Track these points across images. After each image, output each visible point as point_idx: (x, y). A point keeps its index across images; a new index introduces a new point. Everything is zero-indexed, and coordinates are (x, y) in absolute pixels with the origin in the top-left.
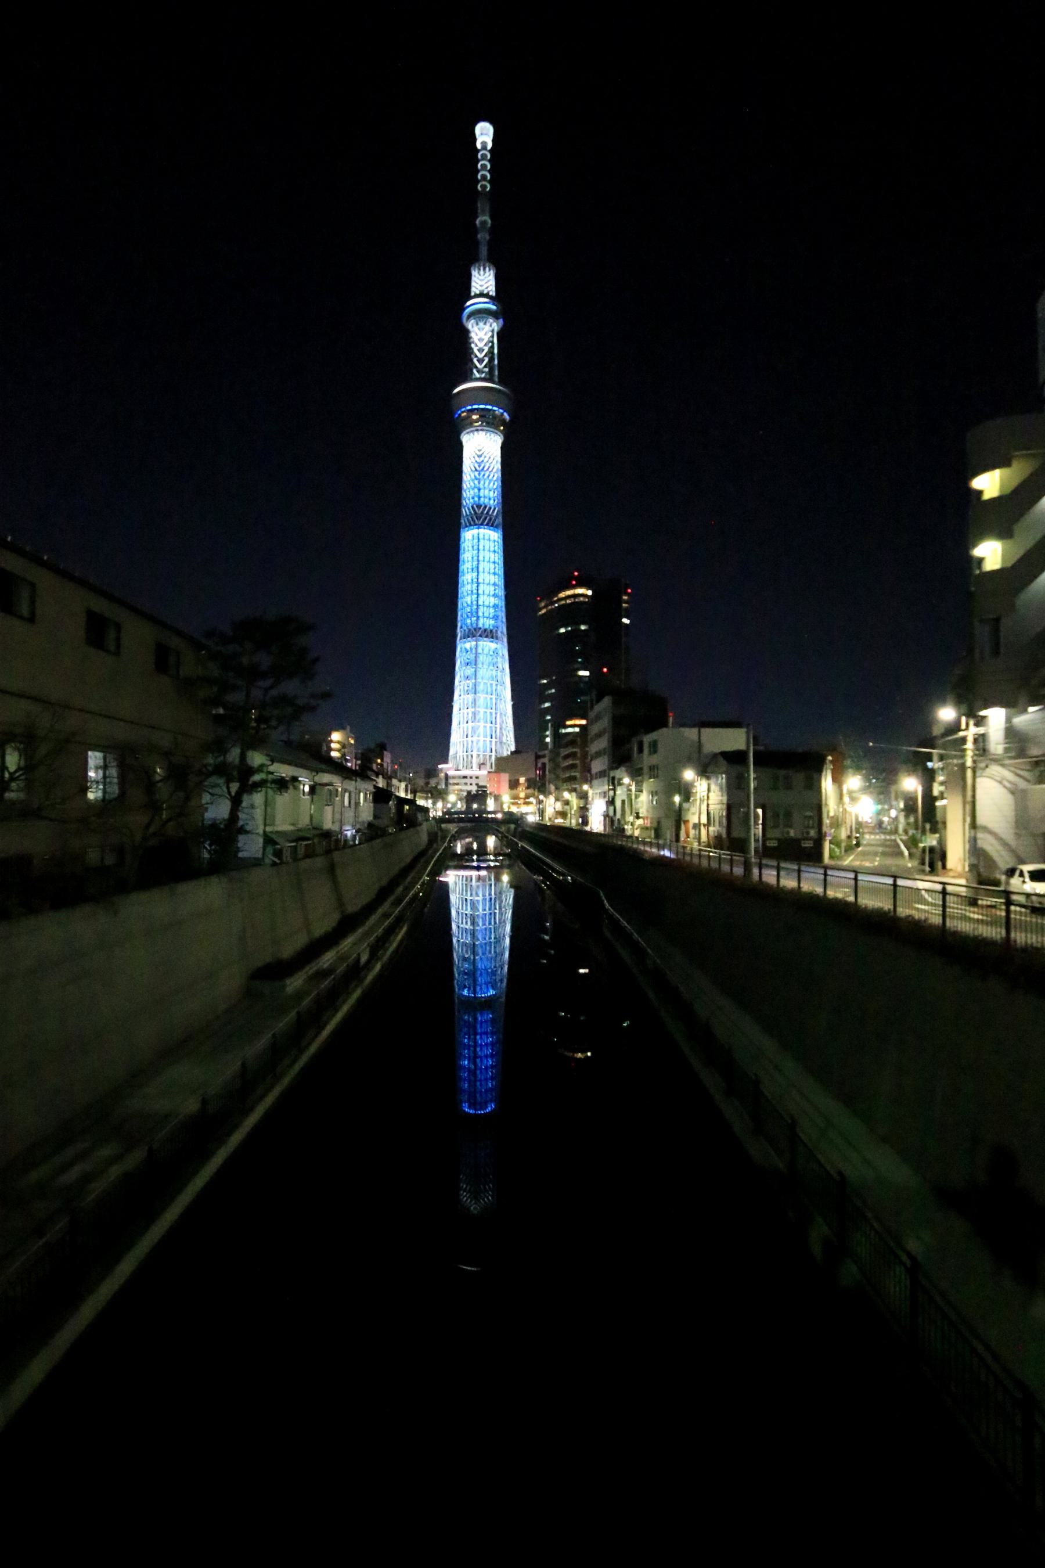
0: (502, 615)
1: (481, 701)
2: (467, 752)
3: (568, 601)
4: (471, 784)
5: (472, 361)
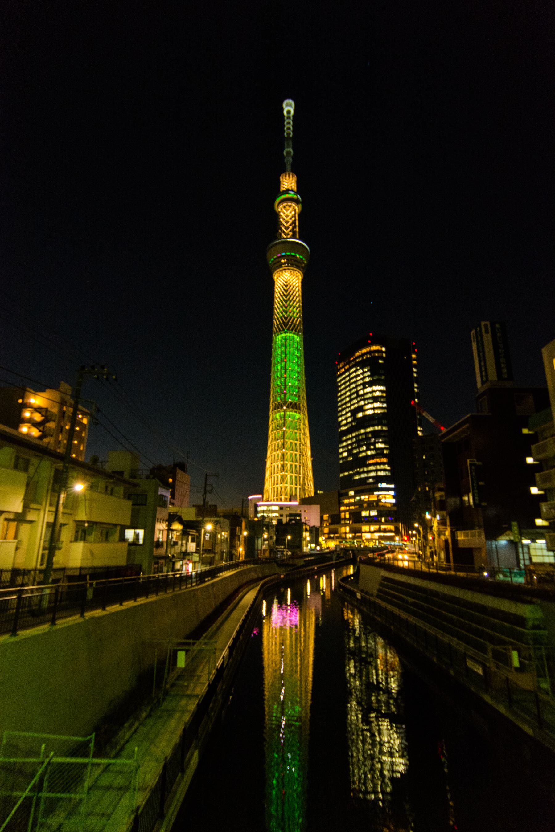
0: (303, 394)
2: (277, 496)
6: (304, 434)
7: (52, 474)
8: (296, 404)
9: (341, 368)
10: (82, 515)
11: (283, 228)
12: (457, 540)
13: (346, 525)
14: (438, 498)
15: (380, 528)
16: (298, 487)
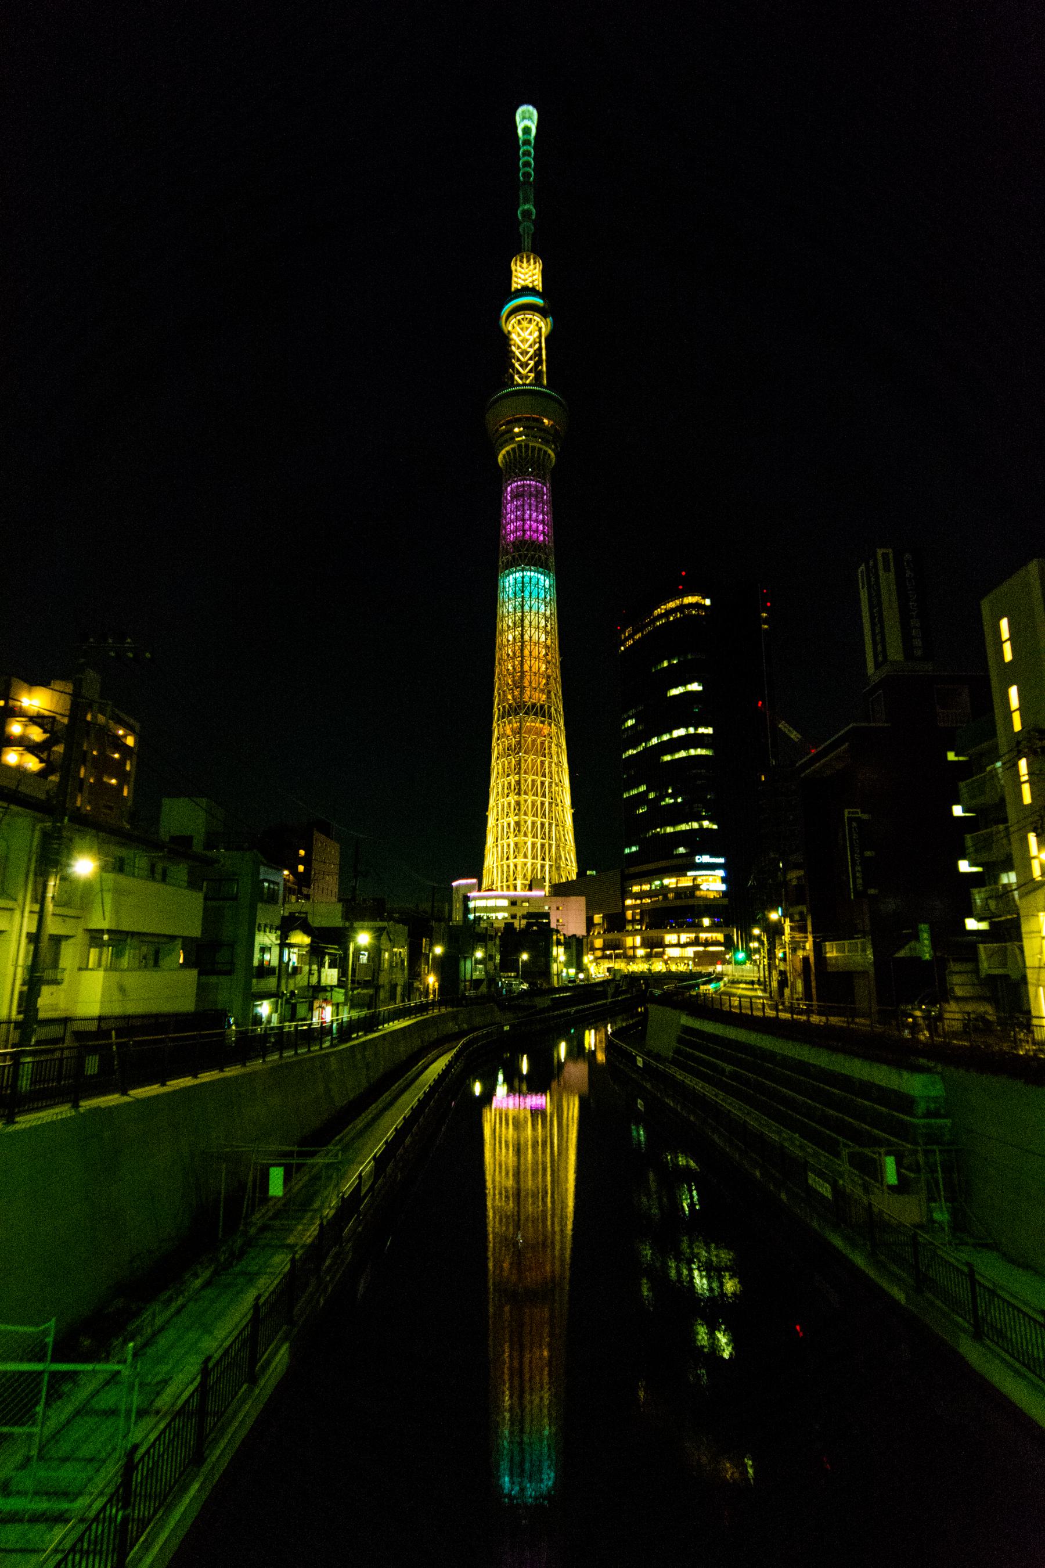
0: (557, 688)
2: (507, 881)
5: (513, 366)
6: (559, 764)
7: (36, 841)
8: (542, 706)
9: (627, 639)
10: (101, 920)
11: (517, 365)
12: (825, 957)
13: (635, 932)
14: (795, 882)
15: (697, 938)
16: (547, 863)
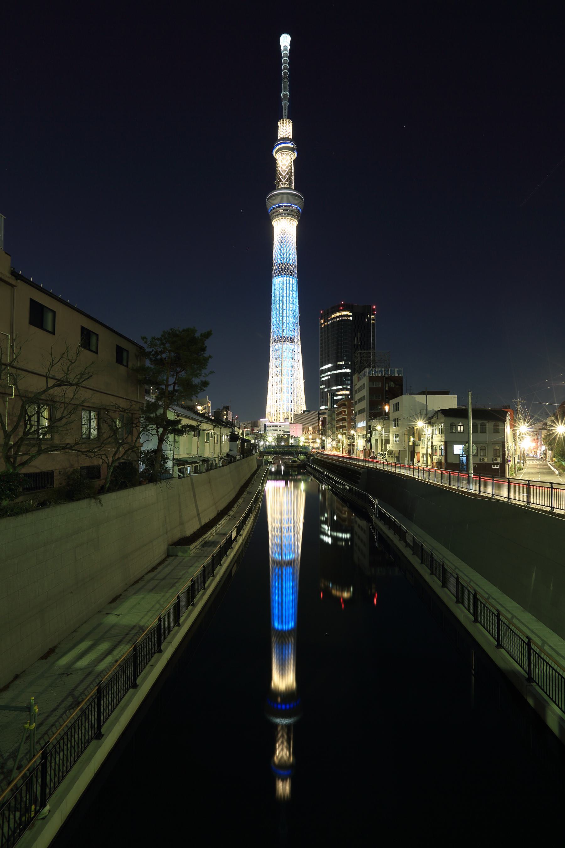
0: (298, 328)
1: (285, 381)
3: (338, 320)
4: (280, 431)
8: (291, 338)
11: (280, 177)
